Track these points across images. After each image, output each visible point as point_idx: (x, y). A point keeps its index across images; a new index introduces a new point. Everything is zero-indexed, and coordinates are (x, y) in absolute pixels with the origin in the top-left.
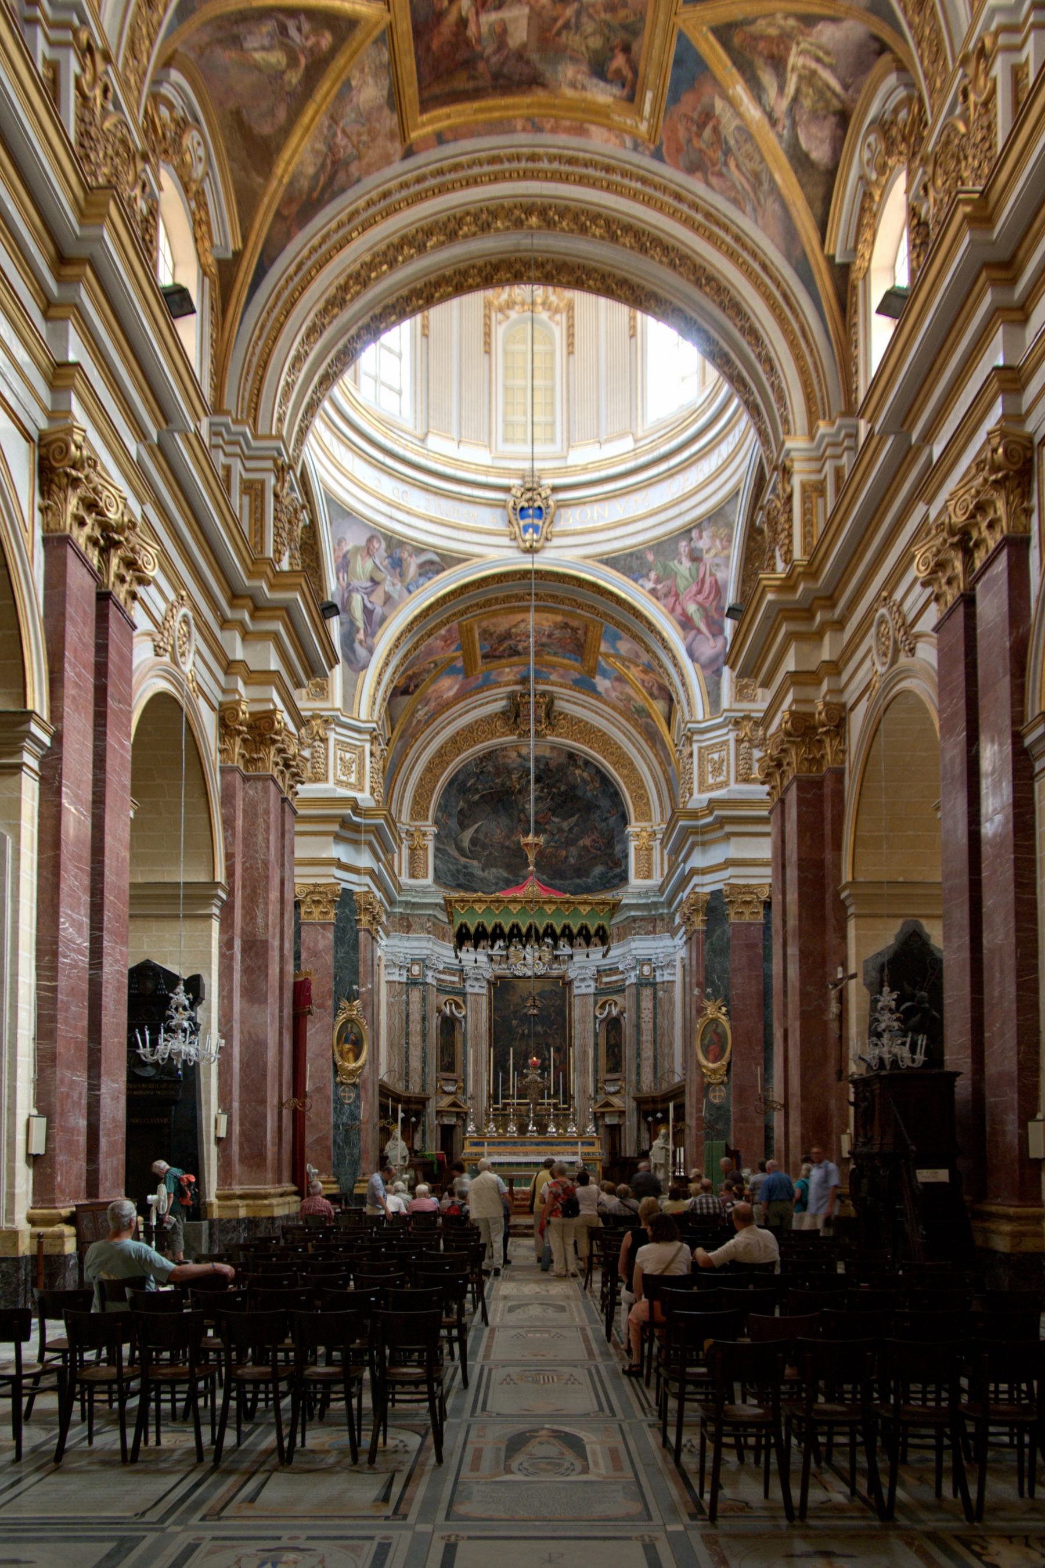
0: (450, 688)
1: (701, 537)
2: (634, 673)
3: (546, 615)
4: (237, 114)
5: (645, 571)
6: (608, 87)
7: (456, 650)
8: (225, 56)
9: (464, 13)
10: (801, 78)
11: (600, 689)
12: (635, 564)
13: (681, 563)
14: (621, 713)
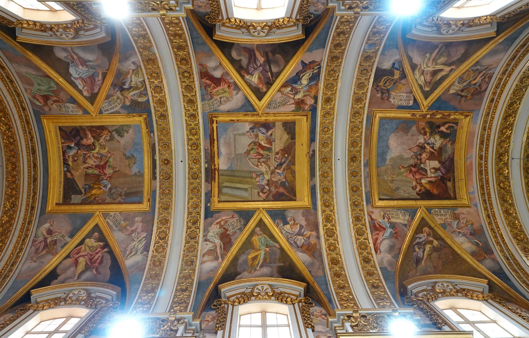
10: (436, 65)
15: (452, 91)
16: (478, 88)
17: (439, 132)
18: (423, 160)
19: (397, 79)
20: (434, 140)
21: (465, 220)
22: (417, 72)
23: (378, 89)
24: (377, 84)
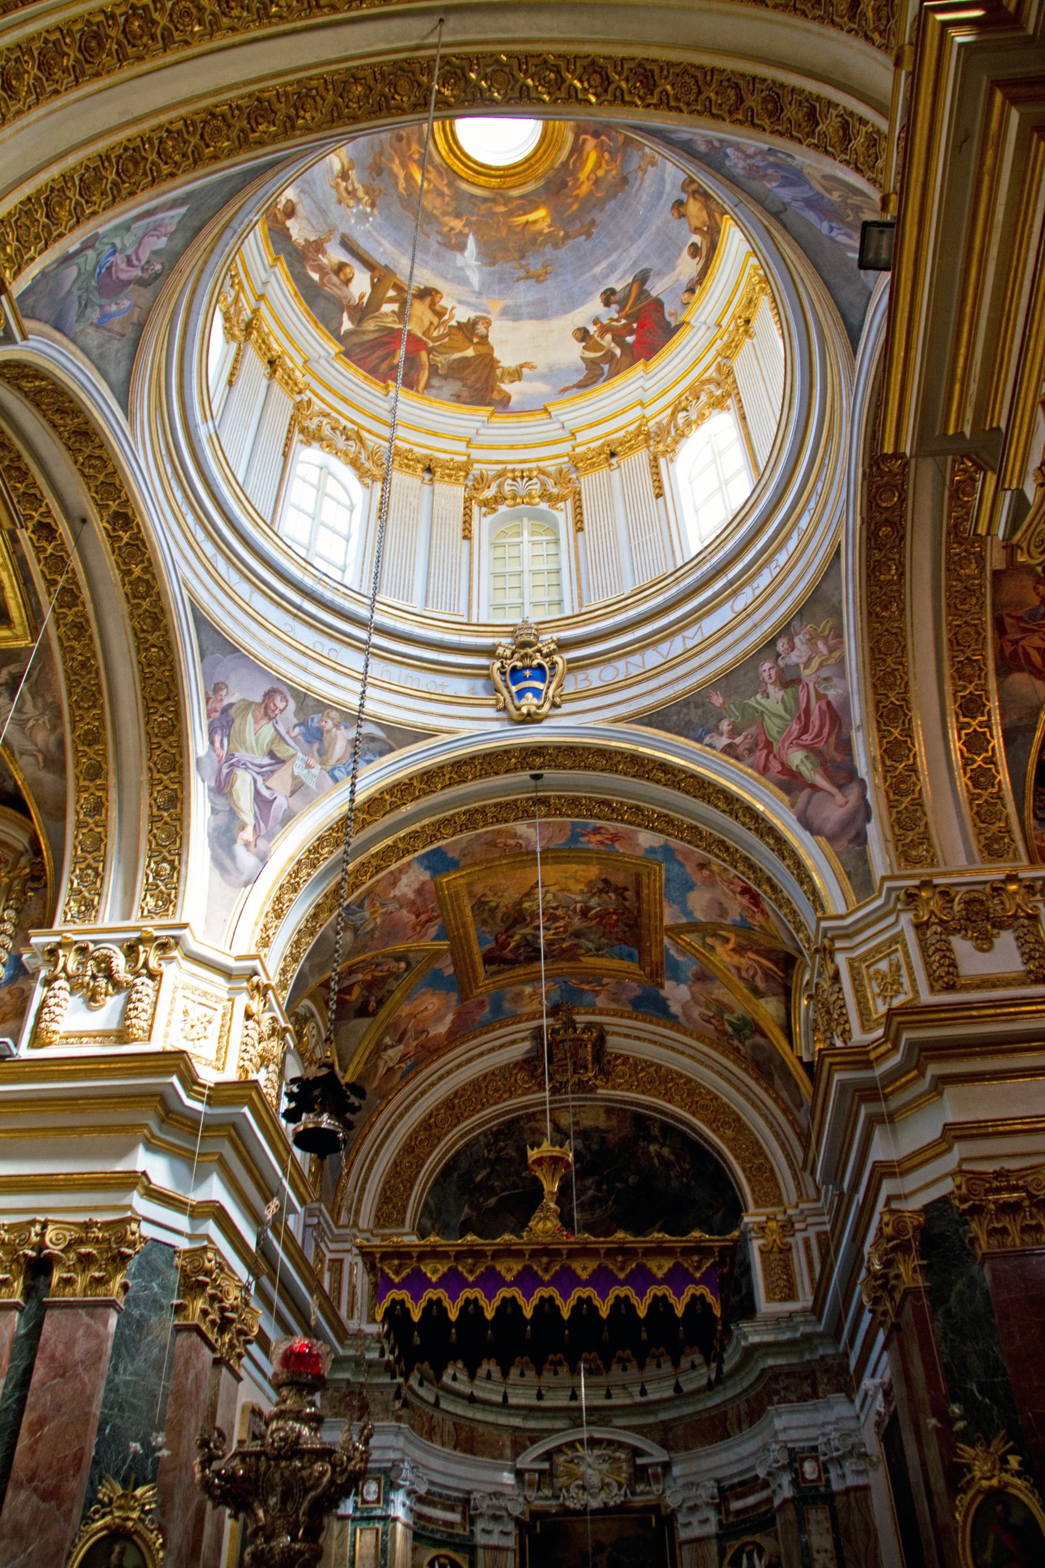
0: (439, 1018)
1: (792, 647)
2: (723, 955)
3: (574, 867)
5: (712, 722)
7: (437, 938)
11: (675, 1008)
12: (694, 715)
13: (768, 697)
14: (710, 1046)
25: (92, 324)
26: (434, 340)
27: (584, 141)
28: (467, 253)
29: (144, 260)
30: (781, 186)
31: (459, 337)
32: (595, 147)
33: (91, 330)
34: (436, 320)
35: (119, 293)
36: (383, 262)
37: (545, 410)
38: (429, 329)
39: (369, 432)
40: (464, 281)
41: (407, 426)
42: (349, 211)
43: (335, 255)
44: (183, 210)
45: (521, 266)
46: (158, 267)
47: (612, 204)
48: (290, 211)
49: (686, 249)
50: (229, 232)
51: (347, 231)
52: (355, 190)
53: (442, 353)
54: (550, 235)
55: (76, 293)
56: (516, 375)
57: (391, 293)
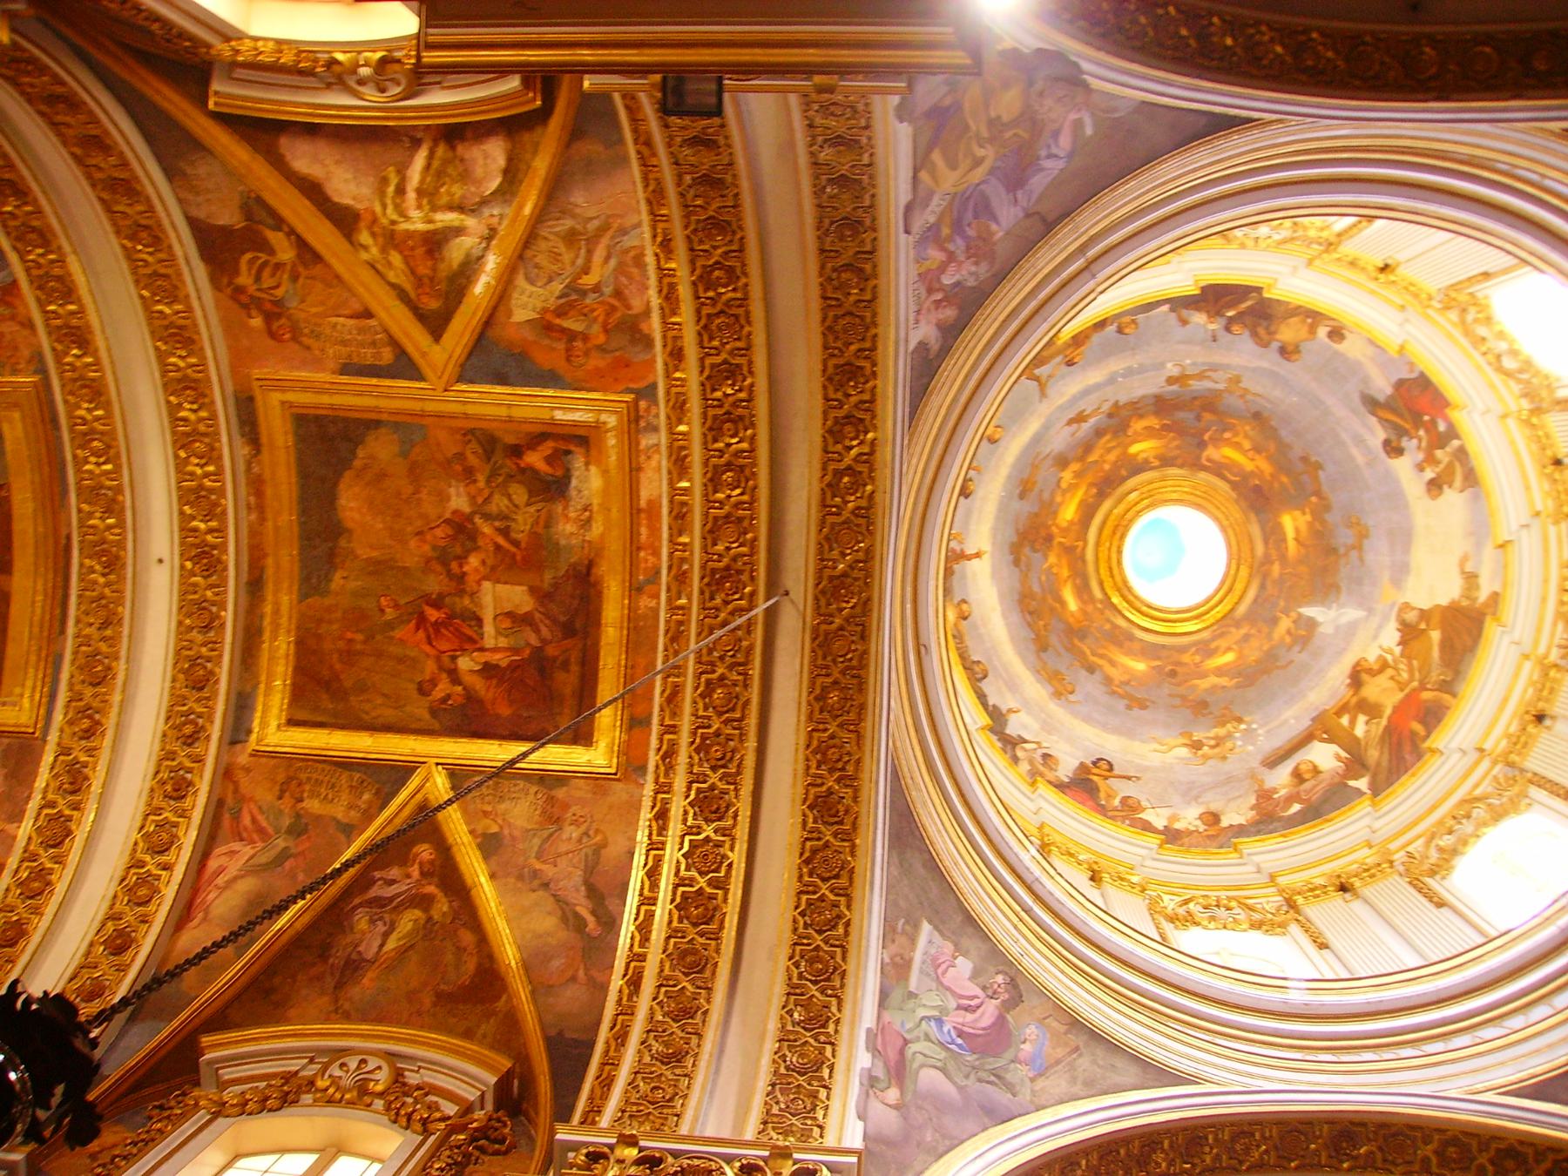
4: (440, 997)
6: (576, 473)
8: (366, 985)
9: (477, 668)
10: (434, 209)
15: (520, 315)
16: (616, 303)
17: (523, 471)
18: (471, 580)
19: (294, 265)
20: (506, 501)
21: (583, 828)
22: (364, 237)
23: (244, 299)
24: (230, 283)
25: (1032, 1080)
26: (1411, 680)
27: (1209, 460)
28: (1320, 619)
29: (979, 992)
30: (995, 219)
31: (1416, 645)
32: (1217, 447)
33: (1040, 1084)
34: (1390, 672)
35: (1010, 1034)
36: (1306, 723)
37: (1501, 546)
38: (1399, 682)
39: (1477, 785)
40: (1352, 629)
41: (1487, 734)
42: (1237, 750)
43: (1280, 778)
44: (926, 927)
45: (1346, 554)
46: (1000, 979)
47: (1283, 433)
48: (1213, 818)
49: (1336, 346)
50: (1036, 887)
51: (1259, 757)
52: (1216, 738)
53: (1429, 672)
54: (1312, 513)
55: (971, 1082)
56: (1471, 579)
57: (1345, 720)
